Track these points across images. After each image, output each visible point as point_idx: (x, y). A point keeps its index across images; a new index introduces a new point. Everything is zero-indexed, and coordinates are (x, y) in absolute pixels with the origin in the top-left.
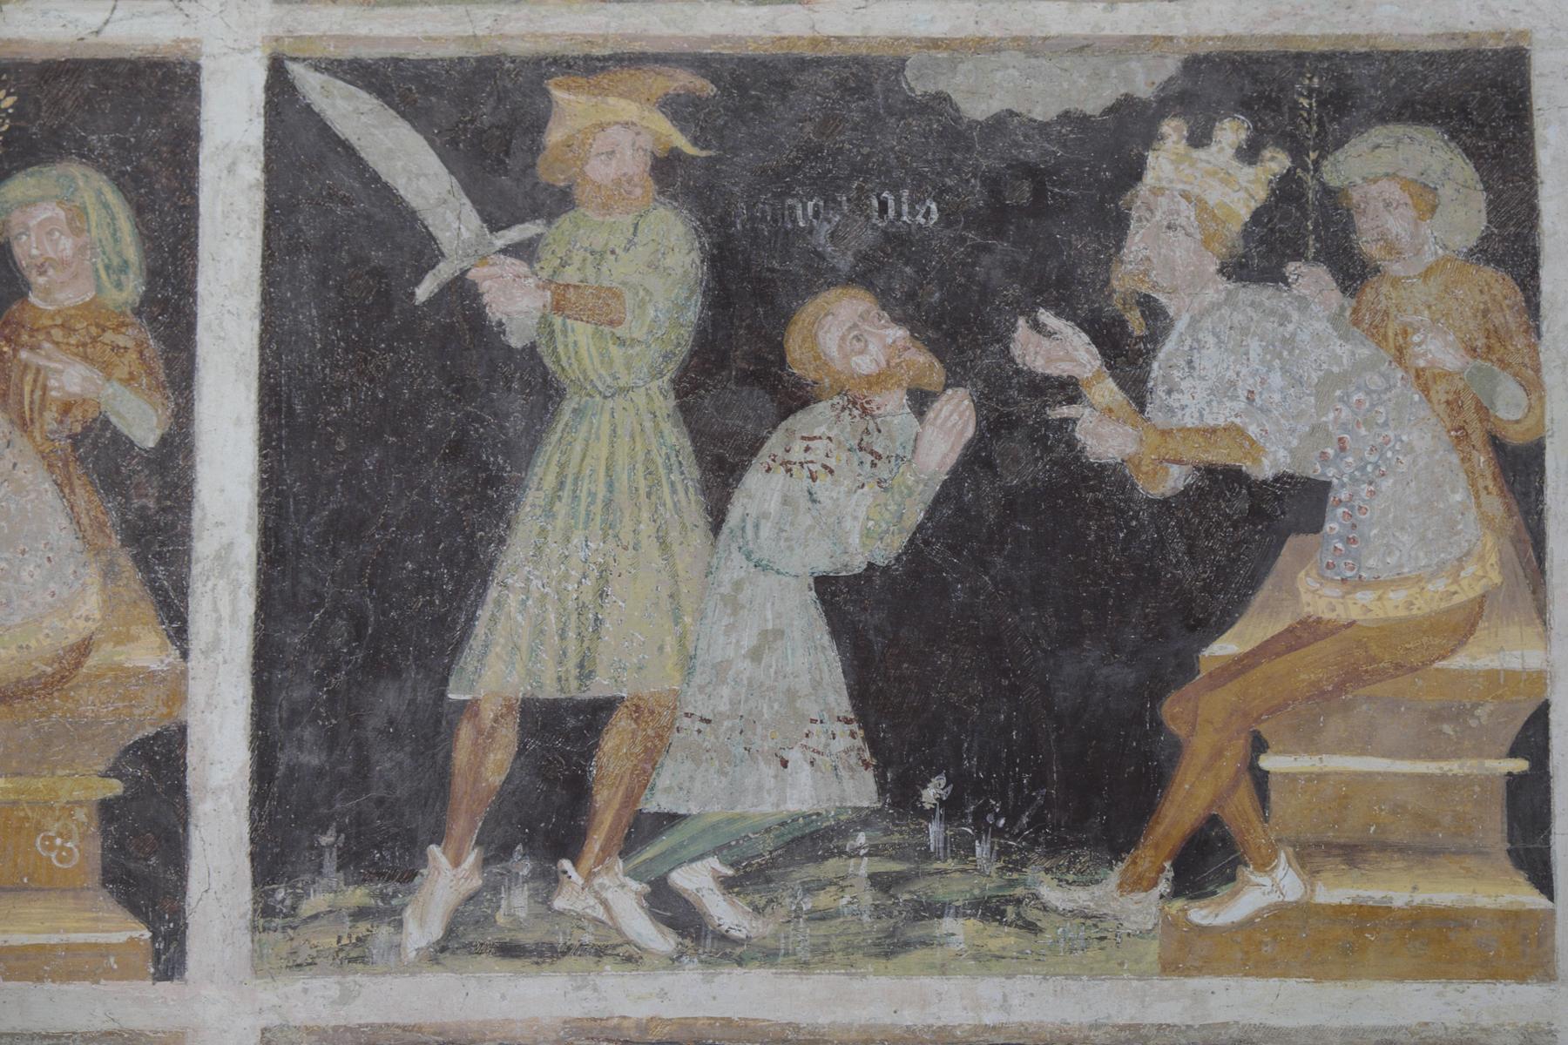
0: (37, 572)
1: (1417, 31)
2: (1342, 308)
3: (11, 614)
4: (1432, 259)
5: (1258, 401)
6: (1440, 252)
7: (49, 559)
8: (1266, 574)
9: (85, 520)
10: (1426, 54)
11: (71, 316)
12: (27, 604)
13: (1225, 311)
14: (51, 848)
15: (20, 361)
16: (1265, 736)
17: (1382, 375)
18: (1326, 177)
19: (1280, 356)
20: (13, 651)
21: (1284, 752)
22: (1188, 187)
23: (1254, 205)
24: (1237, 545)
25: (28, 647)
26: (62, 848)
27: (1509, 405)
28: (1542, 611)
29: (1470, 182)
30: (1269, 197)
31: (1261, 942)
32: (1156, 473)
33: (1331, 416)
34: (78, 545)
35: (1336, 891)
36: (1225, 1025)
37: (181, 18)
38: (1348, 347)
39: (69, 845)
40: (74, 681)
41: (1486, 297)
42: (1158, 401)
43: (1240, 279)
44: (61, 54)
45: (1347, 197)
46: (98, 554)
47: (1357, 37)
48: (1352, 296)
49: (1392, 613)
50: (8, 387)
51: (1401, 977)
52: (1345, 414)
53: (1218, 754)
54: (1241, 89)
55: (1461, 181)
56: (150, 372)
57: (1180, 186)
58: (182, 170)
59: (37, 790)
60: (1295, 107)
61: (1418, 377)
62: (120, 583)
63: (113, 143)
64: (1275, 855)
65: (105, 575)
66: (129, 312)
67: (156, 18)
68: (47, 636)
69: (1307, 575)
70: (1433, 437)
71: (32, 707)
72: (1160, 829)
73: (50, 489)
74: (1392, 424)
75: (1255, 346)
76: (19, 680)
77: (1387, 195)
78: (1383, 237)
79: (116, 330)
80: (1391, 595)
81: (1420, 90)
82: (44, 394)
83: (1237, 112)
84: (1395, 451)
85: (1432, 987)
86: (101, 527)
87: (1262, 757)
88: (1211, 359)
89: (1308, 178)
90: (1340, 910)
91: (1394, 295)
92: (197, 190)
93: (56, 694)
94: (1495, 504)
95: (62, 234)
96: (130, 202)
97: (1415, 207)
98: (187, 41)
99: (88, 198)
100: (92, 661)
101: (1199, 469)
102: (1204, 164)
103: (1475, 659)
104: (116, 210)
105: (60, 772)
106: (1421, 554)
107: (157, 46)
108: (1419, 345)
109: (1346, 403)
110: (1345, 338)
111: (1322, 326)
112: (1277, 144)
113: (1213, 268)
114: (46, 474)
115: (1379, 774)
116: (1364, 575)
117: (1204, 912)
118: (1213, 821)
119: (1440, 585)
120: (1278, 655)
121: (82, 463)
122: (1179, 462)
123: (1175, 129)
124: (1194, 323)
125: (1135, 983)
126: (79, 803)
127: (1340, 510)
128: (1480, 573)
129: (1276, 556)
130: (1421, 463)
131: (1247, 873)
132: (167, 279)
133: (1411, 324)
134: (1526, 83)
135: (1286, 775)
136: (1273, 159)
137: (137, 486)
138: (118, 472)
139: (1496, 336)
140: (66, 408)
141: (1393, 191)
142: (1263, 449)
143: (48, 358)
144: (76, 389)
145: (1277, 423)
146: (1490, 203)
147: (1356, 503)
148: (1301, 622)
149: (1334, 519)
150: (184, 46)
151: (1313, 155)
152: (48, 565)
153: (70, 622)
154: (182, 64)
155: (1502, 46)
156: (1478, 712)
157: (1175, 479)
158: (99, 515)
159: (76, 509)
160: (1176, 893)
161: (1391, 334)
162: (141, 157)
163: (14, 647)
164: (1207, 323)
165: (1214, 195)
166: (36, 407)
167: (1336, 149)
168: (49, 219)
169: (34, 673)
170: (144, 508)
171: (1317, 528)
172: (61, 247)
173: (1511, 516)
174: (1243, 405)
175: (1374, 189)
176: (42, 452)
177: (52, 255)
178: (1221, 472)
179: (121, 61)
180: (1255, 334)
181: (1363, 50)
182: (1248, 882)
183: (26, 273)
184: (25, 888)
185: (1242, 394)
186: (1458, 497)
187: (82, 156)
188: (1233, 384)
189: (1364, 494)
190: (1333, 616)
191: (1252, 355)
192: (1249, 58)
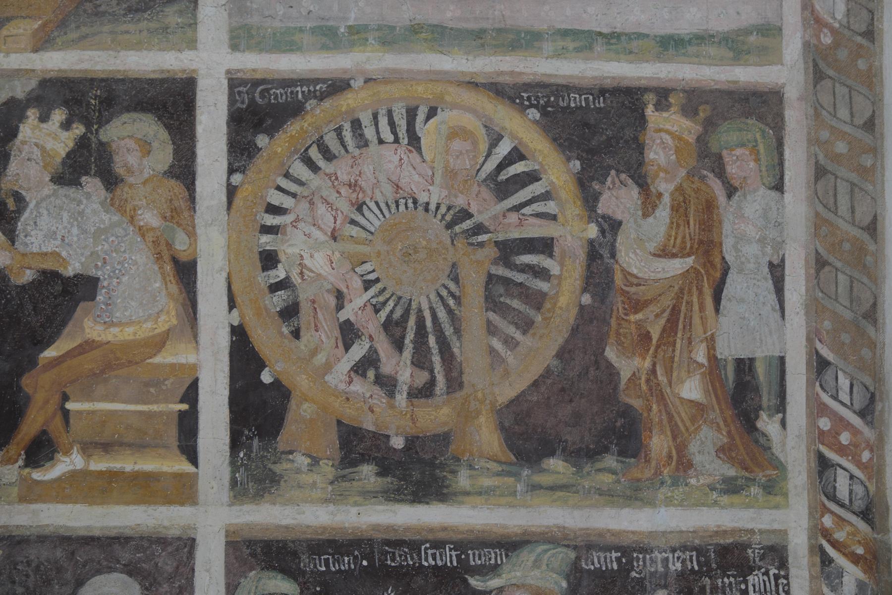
1: (146, 68)
2: (106, 198)
4: (148, 175)
5: (67, 241)
6: (151, 172)
8: (70, 320)
10: (150, 79)
13: (52, 199)
16: (68, 393)
17: (123, 229)
18: (101, 137)
19: (77, 220)
21: (77, 401)
22: (37, 141)
23: (67, 150)
24: (56, 306)
27: (181, 243)
28: (195, 336)
29: (166, 141)
30: (74, 146)
31: (65, 488)
32: (19, 273)
33: (100, 248)
35: (99, 464)
36: (47, 525)
38: (108, 216)
41: (172, 193)
42: (20, 241)
43: (60, 184)
45: (110, 147)
47: (119, 71)
48: (111, 192)
49: (127, 338)
51: (128, 503)
52: (106, 247)
53: (47, 402)
54: (65, 95)
55: (162, 139)
57: (34, 140)
60: (89, 104)
61: (140, 230)
64: (72, 448)
69: (88, 320)
70: (146, 257)
72: (20, 436)
74: (128, 252)
75: (65, 216)
77: (128, 146)
78: (125, 165)
80: (127, 329)
81: (146, 96)
83: (62, 106)
84: (129, 264)
85: (142, 508)
87: (67, 403)
88: (45, 222)
89: (92, 137)
90: (101, 473)
91: (130, 192)
94: (174, 288)
97: (141, 151)
101: (39, 272)
102: (45, 131)
103: (165, 358)
106: (141, 311)
108: (141, 215)
109: (107, 242)
110: (107, 212)
111: (97, 206)
112: (79, 121)
113: (48, 179)
115: (120, 411)
116: (114, 320)
117: (39, 474)
118: (44, 432)
119: (149, 325)
120: (75, 357)
122: (30, 268)
123: (33, 114)
124: (38, 205)
125: (6, 507)
127: (104, 291)
128: (167, 319)
129: (74, 311)
130: (141, 269)
131: (59, 456)
133: (137, 205)
134: (194, 94)
135: (77, 412)
136: (77, 128)
139: (175, 211)
141: (131, 143)
142: (68, 263)
145: (75, 250)
146: (174, 150)
147: (111, 287)
148: (85, 342)
149: (101, 295)
151: (95, 127)
155: (185, 76)
156: (166, 382)
157: (28, 276)
160: (26, 465)
161: (128, 210)
164: (44, 204)
165: (50, 145)
167: (106, 124)
171: (93, 298)
173: (181, 294)
174: (59, 243)
175: (122, 143)
178: (49, 273)
180: (65, 210)
181: (121, 77)
182: (59, 460)
185: (59, 237)
186: (157, 285)
188: (55, 233)
189: (114, 284)
190: (100, 339)
191: (64, 219)
192: (69, 80)
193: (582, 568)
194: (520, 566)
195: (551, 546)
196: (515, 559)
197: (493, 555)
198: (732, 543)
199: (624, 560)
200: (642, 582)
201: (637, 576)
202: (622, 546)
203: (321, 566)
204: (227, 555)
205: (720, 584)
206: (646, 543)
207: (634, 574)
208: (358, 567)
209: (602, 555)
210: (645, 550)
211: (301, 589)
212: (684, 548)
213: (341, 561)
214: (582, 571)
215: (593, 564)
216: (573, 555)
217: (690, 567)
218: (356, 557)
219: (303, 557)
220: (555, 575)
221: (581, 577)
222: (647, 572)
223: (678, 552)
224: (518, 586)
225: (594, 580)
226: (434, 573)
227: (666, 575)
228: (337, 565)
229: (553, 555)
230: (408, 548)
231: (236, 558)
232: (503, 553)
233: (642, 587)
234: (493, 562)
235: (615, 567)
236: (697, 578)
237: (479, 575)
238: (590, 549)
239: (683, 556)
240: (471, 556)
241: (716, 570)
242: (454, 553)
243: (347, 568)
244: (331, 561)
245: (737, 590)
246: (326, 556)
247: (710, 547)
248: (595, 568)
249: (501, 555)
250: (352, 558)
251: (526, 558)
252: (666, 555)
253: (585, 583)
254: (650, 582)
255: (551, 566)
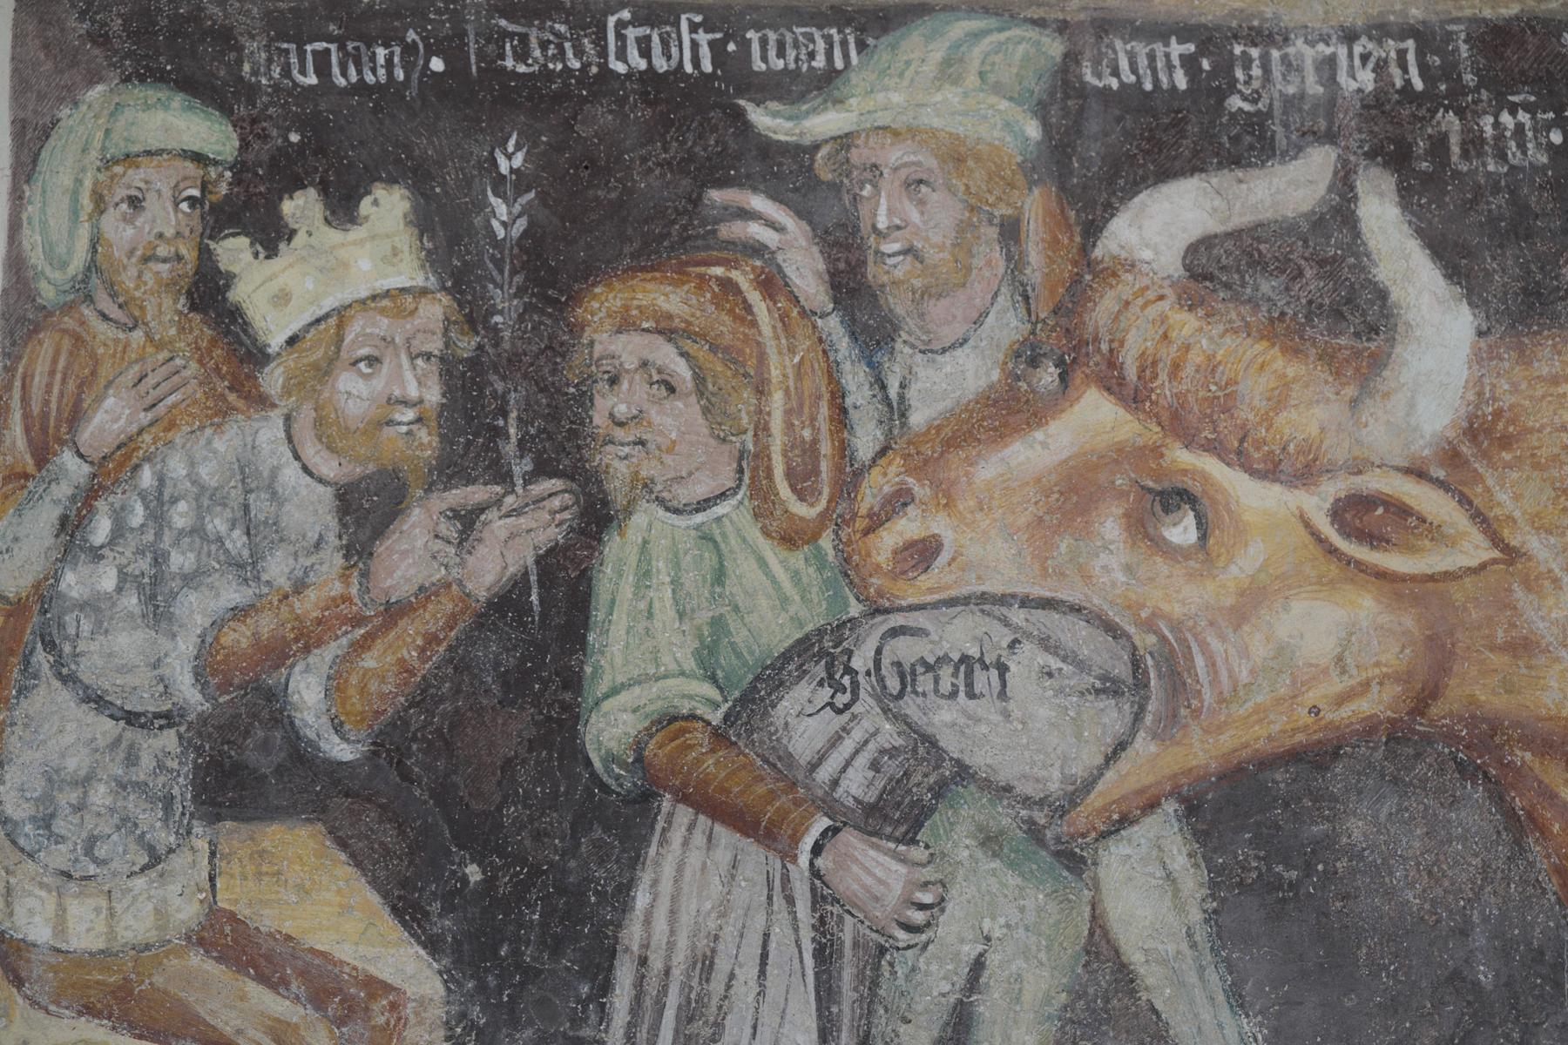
193: (1084, 84)
194: (901, 75)
195: (992, 22)
196: (886, 56)
197: (821, 45)
198: (1518, 18)
199: (1206, 65)
200: (1261, 125)
201: (1247, 107)
202: (1200, 26)
203: (303, 72)
204: (18, 38)
205: (1489, 131)
206: (1269, 15)
207: (1235, 103)
208: (415, 76)
209: (1141, 49)
210: (1264, 36)
211: (242, 139)
212: (1380, 30)
213: (365, 59)
214: (1083, 92)
215: (1116, 73)
216: (1055, 48)
217: (1399, 83)
218: (409, 49)
219: (251, 46)
220: (1004, 105)
221: (1082, 109)
222: (1276, 95)
223: (1364, 40)
224: (896, 134)
225: (1119, 120)
226: (644, 95)
227: (1331, 103)
228: (352, 71)
229: (999, 48)
230: (566, 22)
231: (46, 47)
232: (851, 39)
233: (1261, 138)
234: (820, 62)
235: (1181, 82)
236: (1423, 112)
237: (780, 99)
238: (1107, 32)
239: (1378, 53)
240: (756, 48)
241: (1477, 89)
242: (703, 38)
243: (383, 79)
244: (334, 59)
245: (1538, 145)
246: (320, 46)
247: (1454, 28)
248: (1122, 84)
249: (844, 43)
250: (397, 50)
251: (916, 55)
252: (1329, 51)
253: (1093, 126)
254: (1286, 126)
255: (992, 78)
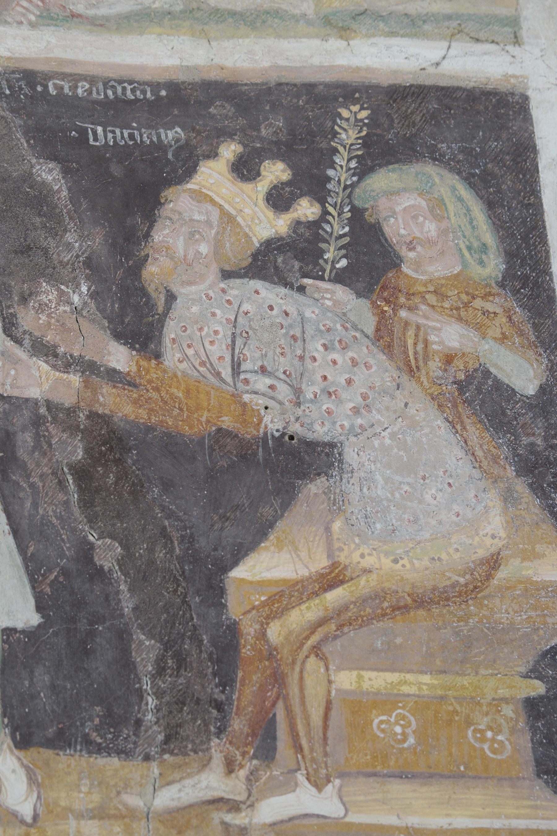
0: (439, 495)
3: (419, 531)
7: (449, 485)
9: (479, 453)
11: (442, 285)
12: (434, 522)
14: (483, 740)
15: (401, 319)
20: (426, 562)
25: (439, 559)
26: (493, 740)
34: (476, 473)
37: (508, 59)
39: (500, 738)
40: (486, 592)
44: (407, 80)
46: (496, 481)
50: (392, 340)
56: (521, 334)
58: (524, 176)
59: (463, 687)
62: (520, 507)
63: (462, 150)
65: (505, 500)
66: (494, 285)
67: (486, 57)
68: (457, 550)
71: (450, 613)
73: (443, 426)
76: (434, 589)
79: (484, 297)
82: (426, 346)
86: (495, 459)
92: (540, 191)
93: (470, 602)
95: (425, 218)
96: (481, 199)
98: (514, 76)
99: (445, 192)
100: (502, 574)
104: (470, 204)
105: (482, 671)
107: (489, 79)
114: (437, 413)
121: (470, 405)
126: (505, 700)
132: (523, 260)
137: (523, 426)
138: (504, 414)
140: (449, 359)
143: (426, 317)
144: (455, 344)
150: (512, 81)
152: (449, 490)
153: (477, 539)
154: (513, 94)
158: (492, 449)
159: (469, 443)
162: (486, 164)
163: (426, 558)
166: (420, 358)
168: (413, 206)
169: (448, 583)
170: (532, 445)
172: (426, 229)
176: (431, 395)
177: (418, 234)
179: (459, 88)
183: (397, 248)
184: (463, 776)
187: (435, 159)
